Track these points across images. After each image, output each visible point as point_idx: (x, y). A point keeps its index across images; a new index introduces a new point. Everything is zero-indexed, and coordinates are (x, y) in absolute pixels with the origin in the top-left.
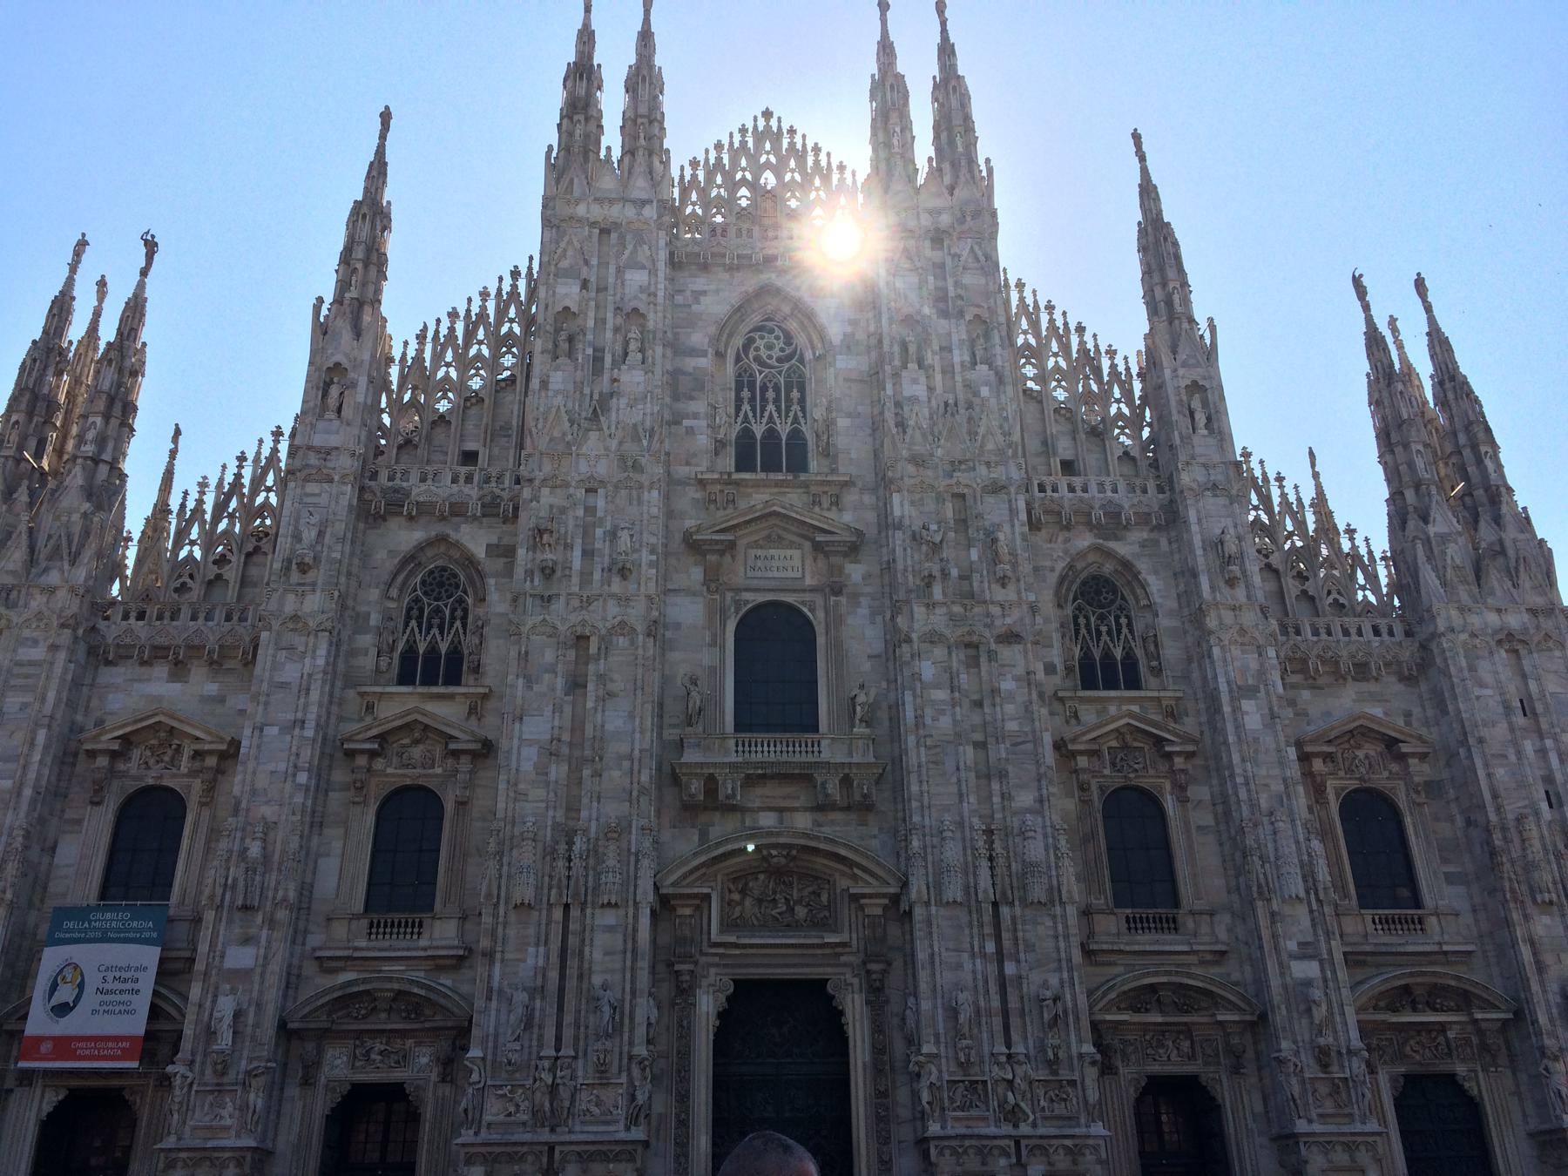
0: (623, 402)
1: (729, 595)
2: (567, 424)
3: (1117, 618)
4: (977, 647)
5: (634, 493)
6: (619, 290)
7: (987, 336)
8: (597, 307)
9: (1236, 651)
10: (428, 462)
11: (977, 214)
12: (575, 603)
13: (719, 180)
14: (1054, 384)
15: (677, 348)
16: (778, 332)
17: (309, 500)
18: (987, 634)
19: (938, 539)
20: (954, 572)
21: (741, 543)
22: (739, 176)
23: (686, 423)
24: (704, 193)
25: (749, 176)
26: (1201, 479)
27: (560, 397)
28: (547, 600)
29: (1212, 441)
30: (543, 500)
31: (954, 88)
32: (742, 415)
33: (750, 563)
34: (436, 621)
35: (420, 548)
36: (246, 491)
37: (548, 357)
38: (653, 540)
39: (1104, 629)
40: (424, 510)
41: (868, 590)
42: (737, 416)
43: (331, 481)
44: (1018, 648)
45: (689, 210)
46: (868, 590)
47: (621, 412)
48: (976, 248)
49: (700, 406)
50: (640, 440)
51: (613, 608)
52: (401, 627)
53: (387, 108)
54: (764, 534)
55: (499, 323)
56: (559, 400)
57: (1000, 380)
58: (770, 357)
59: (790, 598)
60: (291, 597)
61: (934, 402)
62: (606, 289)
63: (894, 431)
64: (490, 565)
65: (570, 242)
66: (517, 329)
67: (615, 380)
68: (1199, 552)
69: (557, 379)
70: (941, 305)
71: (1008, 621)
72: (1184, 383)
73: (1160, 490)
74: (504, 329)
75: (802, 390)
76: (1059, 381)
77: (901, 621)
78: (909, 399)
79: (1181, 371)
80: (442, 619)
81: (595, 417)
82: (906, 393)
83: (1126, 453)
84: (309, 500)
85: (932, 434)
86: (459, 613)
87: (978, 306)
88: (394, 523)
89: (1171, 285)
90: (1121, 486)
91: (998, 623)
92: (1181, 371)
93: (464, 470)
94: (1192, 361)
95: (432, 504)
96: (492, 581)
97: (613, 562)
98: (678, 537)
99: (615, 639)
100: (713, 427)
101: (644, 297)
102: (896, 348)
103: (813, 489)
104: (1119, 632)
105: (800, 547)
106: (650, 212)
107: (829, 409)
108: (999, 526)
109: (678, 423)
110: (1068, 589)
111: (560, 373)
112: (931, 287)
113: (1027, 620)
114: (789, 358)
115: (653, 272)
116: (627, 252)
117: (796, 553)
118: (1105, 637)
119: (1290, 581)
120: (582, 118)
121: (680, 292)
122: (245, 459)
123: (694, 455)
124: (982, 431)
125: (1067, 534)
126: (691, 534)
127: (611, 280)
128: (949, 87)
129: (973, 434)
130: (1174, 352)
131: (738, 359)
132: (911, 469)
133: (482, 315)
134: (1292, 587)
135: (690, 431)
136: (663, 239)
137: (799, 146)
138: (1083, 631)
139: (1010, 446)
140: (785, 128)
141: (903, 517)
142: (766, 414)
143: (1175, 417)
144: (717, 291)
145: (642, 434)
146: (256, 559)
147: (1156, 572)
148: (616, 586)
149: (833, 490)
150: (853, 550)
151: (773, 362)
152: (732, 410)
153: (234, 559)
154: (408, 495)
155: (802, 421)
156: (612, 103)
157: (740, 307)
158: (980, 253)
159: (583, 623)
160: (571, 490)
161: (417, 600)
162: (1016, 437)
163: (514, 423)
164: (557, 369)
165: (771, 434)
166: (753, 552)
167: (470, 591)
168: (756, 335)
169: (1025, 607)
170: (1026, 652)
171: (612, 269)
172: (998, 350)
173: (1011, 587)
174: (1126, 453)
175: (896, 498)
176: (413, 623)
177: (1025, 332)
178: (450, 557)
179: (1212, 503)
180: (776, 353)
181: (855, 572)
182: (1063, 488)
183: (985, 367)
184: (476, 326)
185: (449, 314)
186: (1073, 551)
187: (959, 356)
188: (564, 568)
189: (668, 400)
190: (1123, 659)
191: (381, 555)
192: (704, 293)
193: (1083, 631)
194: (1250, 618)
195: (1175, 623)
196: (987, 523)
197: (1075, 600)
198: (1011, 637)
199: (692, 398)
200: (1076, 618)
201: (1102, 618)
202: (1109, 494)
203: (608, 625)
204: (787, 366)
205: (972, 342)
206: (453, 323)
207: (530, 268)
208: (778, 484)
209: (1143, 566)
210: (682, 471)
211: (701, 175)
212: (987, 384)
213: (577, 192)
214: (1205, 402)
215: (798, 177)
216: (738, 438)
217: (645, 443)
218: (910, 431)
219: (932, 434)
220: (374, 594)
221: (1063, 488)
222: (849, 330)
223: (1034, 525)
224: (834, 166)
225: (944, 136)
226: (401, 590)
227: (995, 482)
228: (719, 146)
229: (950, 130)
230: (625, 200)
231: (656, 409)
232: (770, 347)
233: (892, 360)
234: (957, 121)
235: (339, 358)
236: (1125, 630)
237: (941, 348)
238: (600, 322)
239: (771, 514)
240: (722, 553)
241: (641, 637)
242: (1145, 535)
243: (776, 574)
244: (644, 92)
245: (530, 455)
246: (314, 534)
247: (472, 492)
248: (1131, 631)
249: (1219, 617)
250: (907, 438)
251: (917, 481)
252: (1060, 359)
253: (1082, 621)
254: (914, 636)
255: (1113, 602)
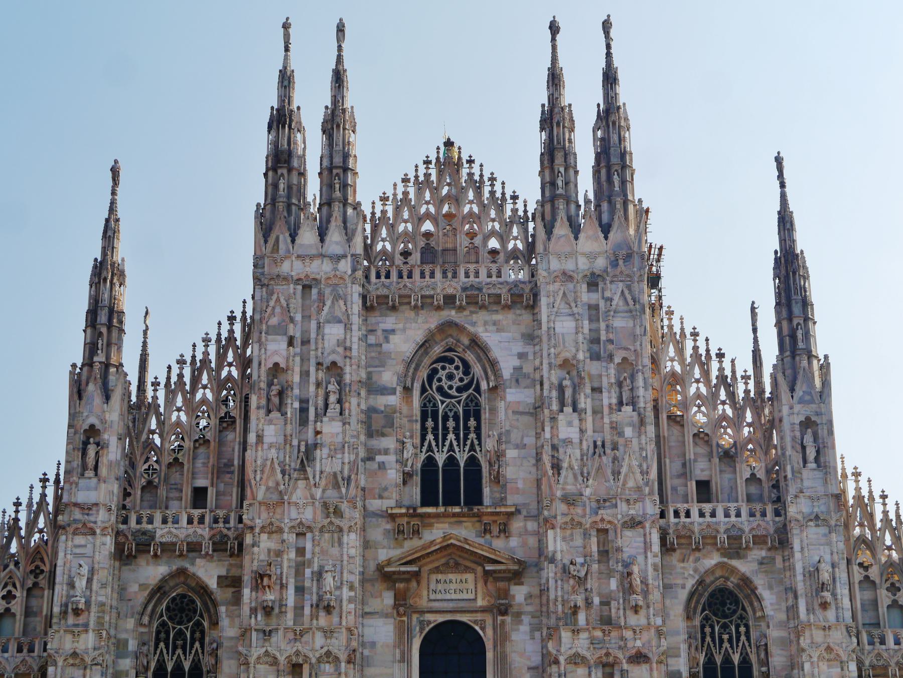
0: (325, 451)
1: (415, 617)
2: (280, 476)
3: (738, 627)
4: (612, 666)
5: (336, 535)
6: (320, 346)
7: (633, 377)
8: (302, 360)
9: (824, 666)
10: (167, 508)
11: (628, 257)
12: (291, 635)
13: (406, 215)
14: (695, 409)
15: (372, 387)
16: (457, 362)
17: (77, 551)
18: (620, 655)
19: (582, 574)
20: (596, 600)
21: (424, 575)
22: (423, 210)
23: (379, 458)
24: (392, 228)
25: (432, 209)
26: (806, 509)
27: (273, 451)
28: (267, 634)
29: (819, 474)
30: (262, 545)
31: (614, 123)
32: (426, 444)
33: (433, 586)
34: (180, 643)
35: (164, 580)
36: (23, 533)
37: (262, 412)
38: (352, 578)
39: (726, 637)
40: (168, 548)
41: (529, 609)
42: (422, 445)
43: (93, 533)
44: (645, 667)
45: (379, 247)
46: (529, 609)
47: (325, 463)
48: (626, 292)
49: (389, 442)
50: (339, 487)
51: (319, 640)
52: (152, 649)
53: (116, 162)
54: (443, 561)
55: (220, 367)
56: (273, 453)
57: (642, 422)
58: (451, 387)
59: (464, 618)
60: (69, 637)
61: (585, 443)
62: (309, 342)
63: (550, 472)
64: (220, 595)
65: (278, 300)
66: (235, 373)
67: (318, 433)
68: (800, 578)
69: (271, 433)
70: (595, 347)
71: (638, 643)
72: (797, 420)
73: (777, 513)
74: (224, 373)
75: (478, 419)
76: (699, 407)
77: (550, 645)
78: (564, 441)
79: (797, 408)
80: (185, 640)
81: (303, 468)
82: (562, 436)
83: (753, 475)
84: (77, 551)
85: (582, 474)
86: (198, 635)
87: (627, 349)
88: (142, 561)
89: (795, 322)
90: (744, 513)
91: (630, 644)
92: (797, 408)
93: (197, 513)
94: (807, 398)
95: (174, 544)
96: (223, 609)
97: (320, 599)
98: (372, 566)
99: (322, 665)
100: (402, 462)
101: (340, 350)
102: (554, 394)
103: (486, 519)
104: (738, 640)
105: (473, 571)
106: (345, 266)
107: (499, 442)
108: (633, 559)
109: (370, 458)
110: (698, 602)
111: (272, 427)
112: (586, 331)
113: (654, 643)
114: (466, 388)
115: (348, 327)
116: (326, 309)
117: (470, 577)
118: (726, 645)
119: (884, 592)
120: (285, 171)
121: (372, 331)
122: (20, 504)
123: (386, 489)
124: (624, 470)
125: (697, 554)
126: (383, 567)
127: (313, 335)
128: (610, 117)
129: (616, 473)
130: (792, 390)
131: (423, 390)
132: (562, 507)
133: (205, 361)
134: (885, 598)
135: (382, 466)
136: (357, 289)
137: (477, 177)
138: (708, 639)
139: (647, 484)
140: (465, 157)
141: (555, 552)
142: (447, 443)
143: (789, 452)
144: (404, 330)
145: (341, 483)
146: (36, 592)
147: (770, 588)
148: (323, 620)
149: (500, 519)
150: (516, 576)
151: (453, 392)
152: (418, 441)
153: (18, 594)
154: (153, 538)
155: (478, 449)
156: (312, 148)
157: (423, 344)
158: (629, 297)
159: (297, 653)
160: (285, 536)
161: (163, 624)
162: (654, 474)
163: (236, 462)
164: (271, 422)
165: (451, 461)
166: (434, 577)
167: (205, 616)
168: (438, 366)
169: (653, 631)
170: (651, 670)
171: (313, 325)
172: (641, 392)
173: (643, 612)
174: (753, 475)
175: (550, 532)
176: (162, 645)
177: (672, 360)
178: (187, 585)
179: (813, 532)
180: (456, 383)
181: (519, 593)
182: (695, 513)
183: (629, 409)
184: (200, 371)
185: (178, 362)
186: (703, 570)
187: (609, 398)
188: (281, 606)
189: (363, 438)
190: (740, 663)
191: (134, 588)
192: (393, 331)
193: (708, 639)
194: (838, 636)
195: (783, 633)
196: (625, 556)
197: (703, 610)
198: (639, 658)
199: (383, 435)
200: (703, 627)
201: (725, 627)
202: (733, 519)
203: (317, 655)
204: (465, 395)
205: (620, 384)
206: (181, 369)
207: (244, 313)
208: (454, 515)
209: (760, 582)
210: (375, 504)
211: (390, 209)
212: (631, 424)
213: (282, 246)
214: (817, 431)
215: (476, 209)
216: (424, 465)
217: (344, 490)
218: (563, 473)
219: (582, 474)
220: (130, 623)
221: (695, 513)
222: (516, 362)
223: (666, 547)
224: (508, 197)
225: (603, 172)
226: (151, 617)
227: (633, 519)
228: (405, 180)
229: (609, 168)
230: (322, 256)
231: (353, 457)
232: (450, 377)
233: (550, 405)
234: (615, 160)
235: (92, 420)
236: (743, 638)
237: (593, 390)
238: (305, 374)
239: (448, 545)
240: (408, 581)
241: (343, 664)
242: (763, 553)
243: (454, 596)
244: (338, 136)
245: (250, 505)
246: (84, 582)
247: (204, 532)
248: (748, 639)
249: (812, 635)
250: (562, 479)
251: (568, 519)
252: (701, 385)
253: (708, 630)
254: (562, 659)
255: (735, 612)
